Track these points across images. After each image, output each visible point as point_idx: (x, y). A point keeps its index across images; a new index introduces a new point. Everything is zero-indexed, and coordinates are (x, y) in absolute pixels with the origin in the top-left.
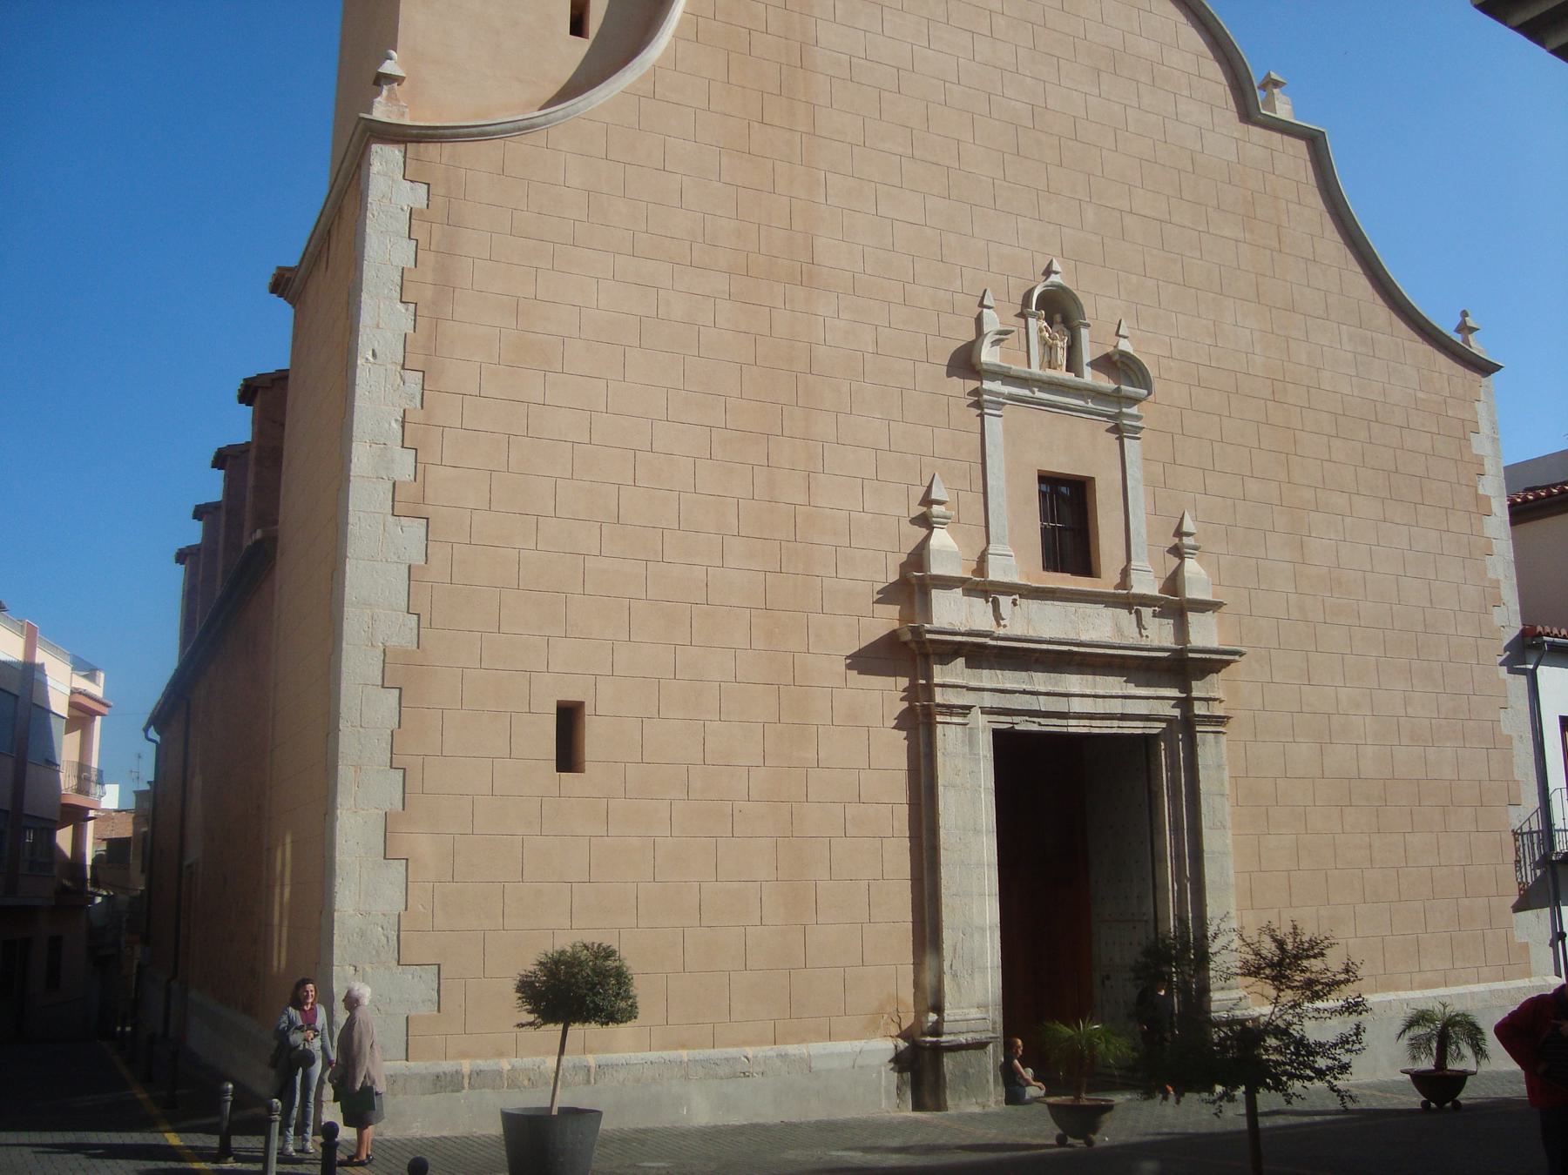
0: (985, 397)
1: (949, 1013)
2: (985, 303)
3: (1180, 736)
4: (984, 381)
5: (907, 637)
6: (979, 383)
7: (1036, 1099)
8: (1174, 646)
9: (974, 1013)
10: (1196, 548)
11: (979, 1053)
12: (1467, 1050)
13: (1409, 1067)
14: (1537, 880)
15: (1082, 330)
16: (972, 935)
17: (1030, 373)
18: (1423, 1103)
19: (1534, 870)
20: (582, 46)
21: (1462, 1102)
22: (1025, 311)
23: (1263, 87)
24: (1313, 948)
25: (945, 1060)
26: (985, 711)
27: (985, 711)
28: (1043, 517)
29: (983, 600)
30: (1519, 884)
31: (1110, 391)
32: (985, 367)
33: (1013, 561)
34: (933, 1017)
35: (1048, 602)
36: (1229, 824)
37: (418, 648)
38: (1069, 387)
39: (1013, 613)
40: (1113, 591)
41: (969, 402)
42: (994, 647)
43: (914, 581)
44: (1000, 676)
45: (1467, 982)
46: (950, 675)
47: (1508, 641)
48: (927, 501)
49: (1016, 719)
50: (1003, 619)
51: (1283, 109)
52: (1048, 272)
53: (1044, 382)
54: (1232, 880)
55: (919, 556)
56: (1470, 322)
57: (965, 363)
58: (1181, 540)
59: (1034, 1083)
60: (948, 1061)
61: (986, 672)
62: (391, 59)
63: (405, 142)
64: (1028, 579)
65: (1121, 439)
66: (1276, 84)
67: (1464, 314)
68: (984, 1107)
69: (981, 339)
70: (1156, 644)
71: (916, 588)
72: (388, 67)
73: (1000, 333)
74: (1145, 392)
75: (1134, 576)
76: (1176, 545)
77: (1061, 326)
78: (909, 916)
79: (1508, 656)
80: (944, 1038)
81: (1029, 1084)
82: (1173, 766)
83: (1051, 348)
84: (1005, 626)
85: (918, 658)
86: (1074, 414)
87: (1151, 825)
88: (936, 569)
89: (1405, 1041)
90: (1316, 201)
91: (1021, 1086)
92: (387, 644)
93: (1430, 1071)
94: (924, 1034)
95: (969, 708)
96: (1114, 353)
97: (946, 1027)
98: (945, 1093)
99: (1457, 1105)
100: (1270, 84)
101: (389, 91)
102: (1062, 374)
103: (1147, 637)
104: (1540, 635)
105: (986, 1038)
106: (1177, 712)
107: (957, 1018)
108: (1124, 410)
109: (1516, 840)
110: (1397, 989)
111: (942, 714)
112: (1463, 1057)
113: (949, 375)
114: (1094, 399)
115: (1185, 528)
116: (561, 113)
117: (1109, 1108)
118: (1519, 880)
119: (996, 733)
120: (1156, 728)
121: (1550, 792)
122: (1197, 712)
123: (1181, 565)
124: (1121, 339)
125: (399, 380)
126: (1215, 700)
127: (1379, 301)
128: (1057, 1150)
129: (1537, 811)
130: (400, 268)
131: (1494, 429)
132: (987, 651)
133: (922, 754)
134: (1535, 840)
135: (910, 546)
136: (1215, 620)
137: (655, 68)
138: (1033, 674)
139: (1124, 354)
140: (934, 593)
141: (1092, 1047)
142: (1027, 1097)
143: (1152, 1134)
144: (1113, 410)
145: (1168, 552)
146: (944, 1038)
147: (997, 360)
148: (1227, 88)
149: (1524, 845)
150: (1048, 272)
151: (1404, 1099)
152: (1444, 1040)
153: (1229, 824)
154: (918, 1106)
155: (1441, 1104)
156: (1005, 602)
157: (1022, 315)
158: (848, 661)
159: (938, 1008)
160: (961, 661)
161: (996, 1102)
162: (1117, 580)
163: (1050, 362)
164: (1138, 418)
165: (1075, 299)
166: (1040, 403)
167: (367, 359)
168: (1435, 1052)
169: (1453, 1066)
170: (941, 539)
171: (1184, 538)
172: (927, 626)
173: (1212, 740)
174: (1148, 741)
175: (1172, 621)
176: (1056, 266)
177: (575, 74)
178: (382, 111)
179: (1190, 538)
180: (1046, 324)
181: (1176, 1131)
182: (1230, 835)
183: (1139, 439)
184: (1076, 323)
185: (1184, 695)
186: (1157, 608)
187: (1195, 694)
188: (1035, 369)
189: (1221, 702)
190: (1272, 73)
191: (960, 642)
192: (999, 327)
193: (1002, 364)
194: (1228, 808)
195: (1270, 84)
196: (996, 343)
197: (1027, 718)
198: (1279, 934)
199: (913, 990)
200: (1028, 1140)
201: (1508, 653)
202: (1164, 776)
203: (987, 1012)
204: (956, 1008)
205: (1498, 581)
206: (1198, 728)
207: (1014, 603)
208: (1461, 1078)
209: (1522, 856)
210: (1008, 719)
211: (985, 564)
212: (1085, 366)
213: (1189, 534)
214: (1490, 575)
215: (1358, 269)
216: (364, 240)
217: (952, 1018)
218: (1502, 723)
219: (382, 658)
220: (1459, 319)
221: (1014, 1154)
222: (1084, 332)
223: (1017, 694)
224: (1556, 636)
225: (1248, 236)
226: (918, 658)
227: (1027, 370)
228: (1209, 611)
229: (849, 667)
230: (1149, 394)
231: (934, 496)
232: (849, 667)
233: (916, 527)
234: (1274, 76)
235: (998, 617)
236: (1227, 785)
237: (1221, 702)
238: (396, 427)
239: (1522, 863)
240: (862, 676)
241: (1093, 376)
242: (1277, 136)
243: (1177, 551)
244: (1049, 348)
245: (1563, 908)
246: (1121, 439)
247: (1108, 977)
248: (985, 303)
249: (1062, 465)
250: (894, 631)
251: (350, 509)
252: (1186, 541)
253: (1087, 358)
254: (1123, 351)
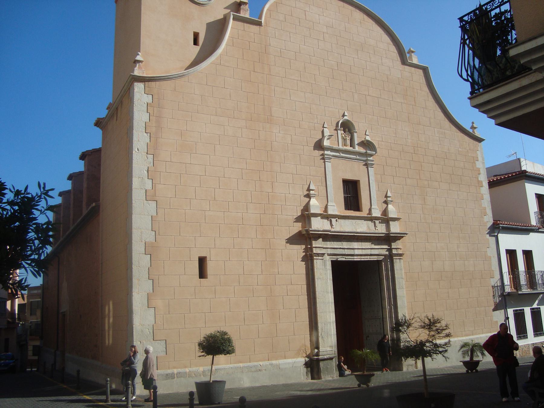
0: (326, 156)
1: (321, 349)
2: (325, 126)
3: (389, 260)
4: (325, 151)
5: (304, 233)
6: (323, 152)
7: (349, 375)
8: (386, 232)
9: (329, 349)
10: (392, 201)
11: (330, 361)
12: (479, 354)
13: (462, 360)
14: (500, 301)
15: (355, 133)
16: (327, 325)
17: (339, 148)
18: (467, 371)
19: (499, 298)
20: (197, 49)
21: (478, 370)
22: (337, 128)
23: (408, 53)
24: (438, 321)
25: (320, 364)
26: (329, 255)
27: (329, 255)
28: (344, 193)
29: (327, 220)
30: (494, 302)
31: (364, 153)
32: (325, 147)
33: (336, 208)
34: (316, 350)
35: (346, 220)
36: (404, 287)
37: (155, 241)
38: (351, 152)
39: (336, 224)
40: (366, 216)
41: (321, 158)
42: (331, 234)
43: (306, 215)
44: (333, 244)
45: (479, 334)
46: (318, 244)
47: (489, 226)
48: (309, 190)
49: (338, 257)
50: (333, 226)
51: (415, 61)
52: (344, 115)
53: (343, 150)
54: (406, 305)
55: (307, 207)
56: (475, 125)
57: (319, 146)
58: (387, 199)
59: (347, 370)
60: (322, 364)
61: (328, 243)
62: (139, 55)
63: (145, 82)
64: (340, 213)
65: (367, 168)
66: (413, 52)
67: (473, 123)
68: (333, 378)
69: (323, 138)
70: (380, 232)
71: (306, 217)
72: (138, 58)
73: (329, 136)
74: (375, 153)
75: (373, 211)
76: (385, 200)
77: (348, 133)
78: (307, 319)
79: (489, 231)
80: (320, 357)
81: (346, 370)
82: (387, 270)
83: (345, 140)
84: (334, 228)
85: (308, 239)
86: (353, 160)
87: (380, 288)
88: (312, 211)
89: (461, 352)
90: (426, 89)
91: (344, 371)
92: (146, 241)
93: (468, 361)
94: (313, 356)
95: (324, 254)
96: (365, 141)
97: (320, 353)
98: (321, 374)
99: (477, 371)
100: (411, 52)
101: (139, 65)
102: (349, 148)
103: (377, 230)
104: (499, 224)
105: (333, 356)
106: (387, 253)
107: (324, 350)
108: (368, 158)
109: (493, 289)
110: (458, 337)
111: (316, 256)
112: (478, 356)
113: (314, 149)
114: (359, 156)
115: (388, 195)
116: (192, 71)
117: (373, 375)
118: (494, 301)
119: (332, 261)
120: (381, 258)
121: (503, 273)
122: (393, 253)
123: (387, 207)
124: (367, 136)
125: (146, 158)
126: (399, 248)
127: (446, 120)
128: (358, 388)
129: (499, 279)
130: (145, 122)
131: (483, 159)
132: (329, 236)
133: (310, 269)
134: (499, 289)
135: (304, 204)
136: (398, 224)
137: (221, 55)
138: (343, 243)
139: (368, 141)
140: (312, 218)
141: (367, 356)
142: (346, 374)
143: (385, 383)
144: (365, 159)
145: (383, 203)
146: (320, 357)
147: (329, 145)
148: (397, 54)
149: (495, 290)
150: (344, 115)
151: (461, 370)
152: (472, 351)
153: (404, 287)
154: (313, 378)
155: (472, 371)
156: (334, 220)
157: (336, 130)
158: (286, 241)
159: (318, 348)
160: (321, 239)
161: (336, 377)
162: (368, 212)
163: (345, 144)
164: (373, 161)
165: (352, 124)
166: (343, 157)
167: (136, 151)
168: (470, 355)
169: (475, 359)
170: (313, 201)
171: (388, 198)
172: (310, 229)
173: (399, 261)
174: (378, 262)
175: (385, 224)
176: (346, 114)
177: (196, 56)
178: (137, 72)
179: (390, 198)
180: (343, 132)
181: (393, 382)
182: (405, 291)
183: (373, 167)
184: (352, 132)
185: (389, 247)
186: (380, 221)
187: (393, 247)
188: (341, 147)
189: (401, 249)
190: (411, 48)
191: (320, 234)
192: (329, 134)
193: (330, 146)
194: (404, 282)
195: (411, 52)
196: (328, 139)
197: (341, 256)
198: (429, 318)
199: (310, 342)
200: (348, 386)
201: (489, 230)
202: (384, 273)
203: (333, 348)
204: (323, 348)
205: (485, 208)
206: (394, 258)
207: (336, 221)
208: (478, 362)
209: (495, 294)
210: (336, 257)
211: (327, 209)
212: (356, 145)
213: (389, 197)
214: (483, 206)
215: (440, 110)
216: (133, 113)
217: (322, 351)
218: (488, 252)
219: (145, 245)
220: (471, 125)
221: (346, 390)
222: (355, 134)
223: (338, 249)
224: (504, 224)
225: (405, 101)
226: (308, 239)
227: (338, 147)
228: (396, 221)
229: (287, 243)
230: (376, 153)
231: (311, 188)
232: (287, 243)
233: (306, 198)
234: (412, 49)
235: (332, 225)
236: (403, 275)
237: (401, 249)
238: (146, 172)
239: (495, 296)
240: (291, 245)
241: (358, 148)
242: (413, 69)
243: (386, 202)
244: (344, 140)
245: (508, 310)
246: (367, 168)
247: (368, 337)
248: (325, 126)
249: (350, 177)
250: (300, 231)
251: (133, 199)
252: (389, 199)
253: (356, 142)
254: (367, 140)
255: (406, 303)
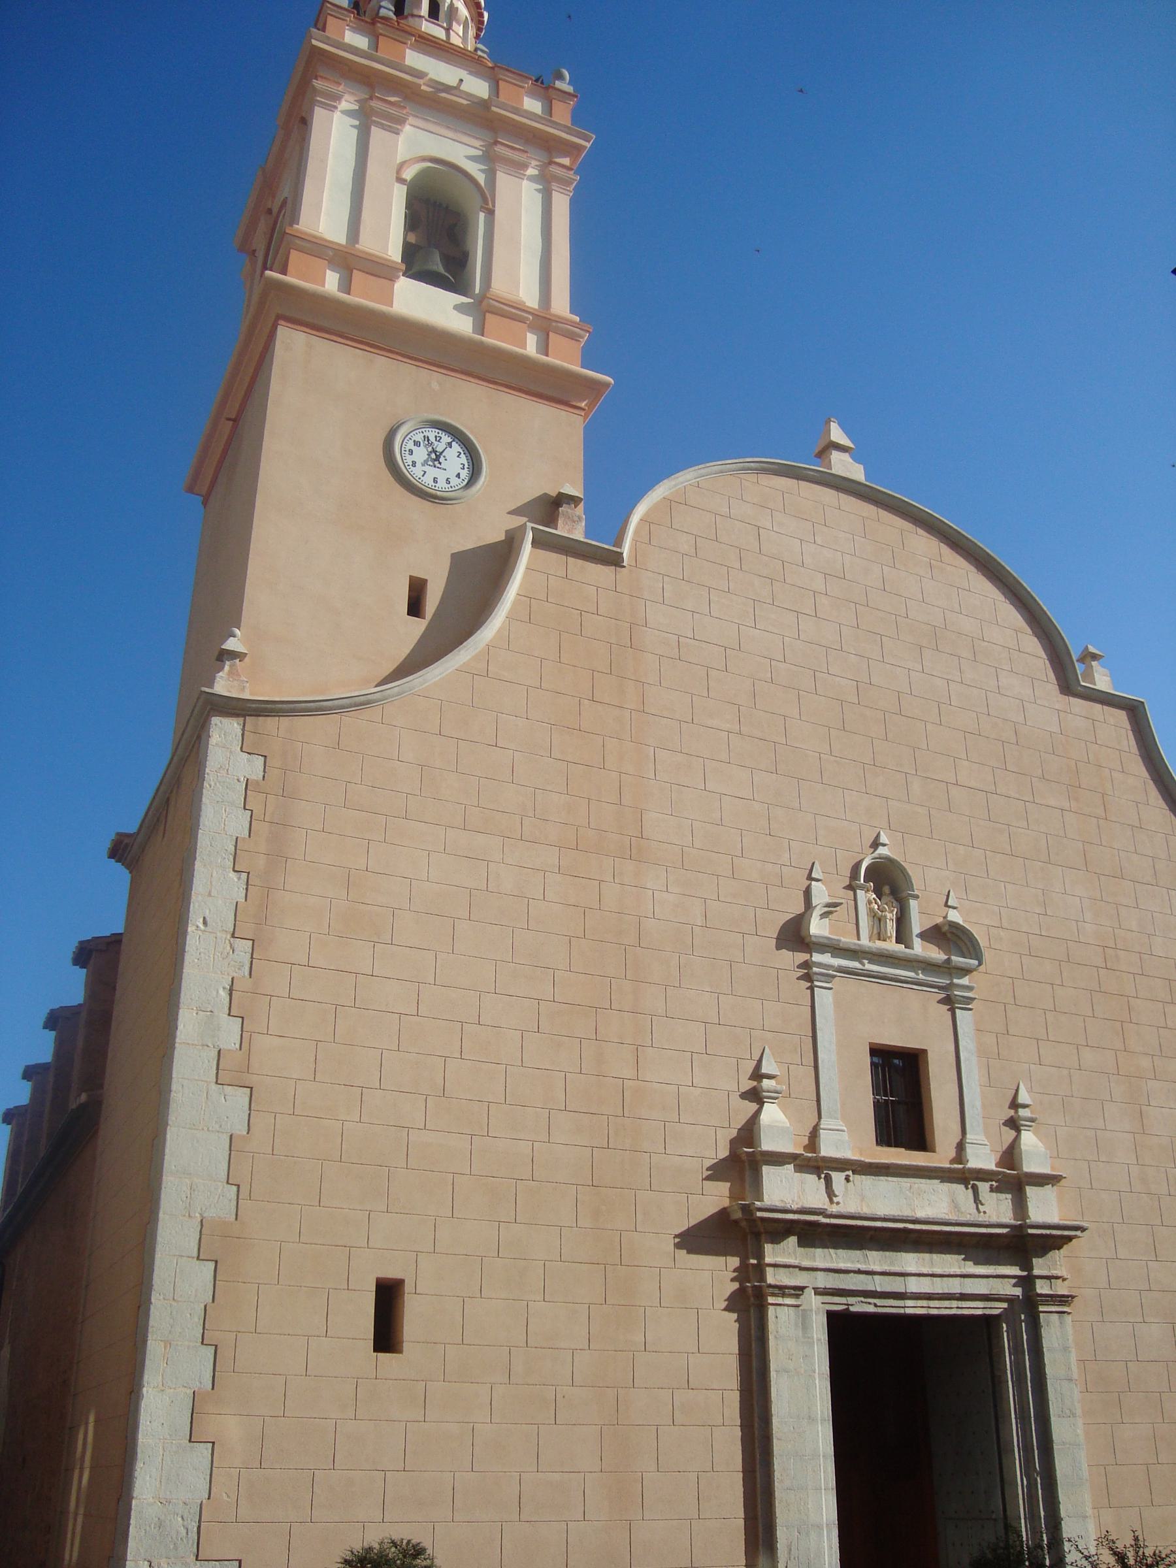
0: (815, 969)
2: (814, 875)
3: (1023, 1317)
4: (813, 954)
5: (738, 1215)
8: (1013, 1222)
10: (1032, 1120)
16: (808, 1534)
17: (859, 945)
20: (418, 626)
22: (853, 883)
23: (1081, 660)
26: (818, 1292)
27: (818, 1292)
28: (876, 1090)
29: (814, 1177)
32: (814, 939)
35: (882, 1178)
36: (1079, 1412)
37: (236, 1219)
39: (846, 1188)
40: (949, 1166)
41: (799, 974)
42: (827, 1225)
43: (744, 1157)
44: (834, 1256)
48: (757, 1075)
49: (851, 1300)
50: (836, 1196)
51: (1102, 681)
52: (876, 844)
55: (749, 1132)
58: (1016, 1112)
61: (819, 1251)
62: (234, 636)
63: (244, 716)
64: (861, 1155)
65: (952, 1011)
66: (1095, 657)
70: (994, 1219)
71: (746, 1164)
72: (231, 644)
73: (828, 905)
74: (976, 962)
75: (970, 1150)
76: (1012, 1117)
77: (890, 898)
82: (1017, 1350)
83: (880, 920)
84: (838, 1203)
86: (905, 985)
92: (204, 1216)
95: (802, 1289)
96: (943, 924)
101: (230, 666)
102: (892, 946)
103: (985, 1212)
106: (1018, 1291)
108: (956, 981)
111: (773, 1295)
113: (778, 947)
114: (924, 971)
116: (396, 690)
119: (831, 1315)
120: (998, 1308)
122: (1039, 1291)
123: (1017, 1139)
125: (228, 948)
126: (1057, 1278)
130: (235, 838)
132: (820, 1230)
133: (753, 1338)
135: (740, 1121)
138: (869, 1253)
139: (954, 926)
140: (766, 1170)
144: (944, 981)
147: (826, 933)
148: (1047, 662)
150: (876, 844)
153: (1079, 1412)
156: (838, 1178)
157: (851, 887)
158: (677, 1240)
164: (969, 988)
165: (903, 871)
167: (197, 927)
170: (771, 1114)
171: (1020, 1110)
173: (1057, 1323)
174: (988, 1323)
176: (884, 839)
177: (413, 650)
178: (223, 685)
179: (1027, 1109)
180: (874, 896)
183: (970, 1009)
184: (904, 894)
185: (1025, 1273)
186: (994, 1183)
187: (1036, 1272)
188: (865, 942)
189: (1064, 1280)
190: (1089, 646)
192: (828, 900)
193: (830, 936)
194: (1076, 1394)
196: (824, 915)
197: (862, 1299)
202: (1008, 1359)
206: (1041, 1308)
207: (847, 1179)
211: (817, 1139)
212: (914, 937)
213: (1025, 1106)
216: (199, 809)
219: (199, 1229)
222: (913, 903)
226: (749, 1237)
228: (1048, 1184)
229: (678, 1246)
230: (980, 964)
231: (764, 1070)
232: (678, 1246)
234: (1092, 649)
235: (830, 1193)
237: (1064, 1280)
238: (224, 995)
241: (924, 948)
242: (1098, 707)
243: (1013, 1124)
246: (952, 1011)
248: (814, 875)
251: (174, 1075)
252: (1022, 1112)
253: (916, 929)
255: (1085, 1466)
